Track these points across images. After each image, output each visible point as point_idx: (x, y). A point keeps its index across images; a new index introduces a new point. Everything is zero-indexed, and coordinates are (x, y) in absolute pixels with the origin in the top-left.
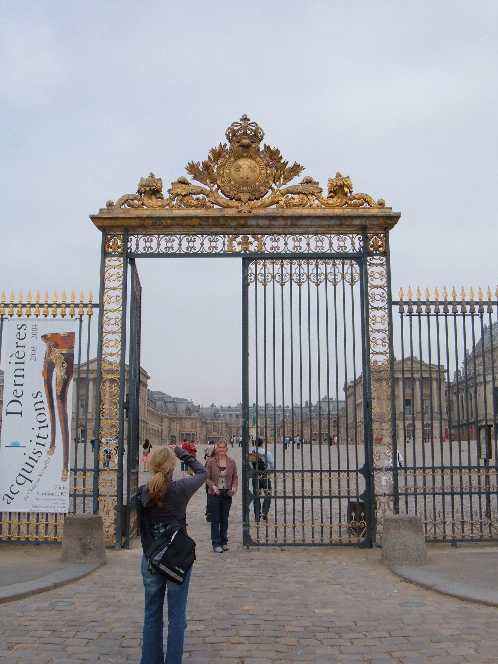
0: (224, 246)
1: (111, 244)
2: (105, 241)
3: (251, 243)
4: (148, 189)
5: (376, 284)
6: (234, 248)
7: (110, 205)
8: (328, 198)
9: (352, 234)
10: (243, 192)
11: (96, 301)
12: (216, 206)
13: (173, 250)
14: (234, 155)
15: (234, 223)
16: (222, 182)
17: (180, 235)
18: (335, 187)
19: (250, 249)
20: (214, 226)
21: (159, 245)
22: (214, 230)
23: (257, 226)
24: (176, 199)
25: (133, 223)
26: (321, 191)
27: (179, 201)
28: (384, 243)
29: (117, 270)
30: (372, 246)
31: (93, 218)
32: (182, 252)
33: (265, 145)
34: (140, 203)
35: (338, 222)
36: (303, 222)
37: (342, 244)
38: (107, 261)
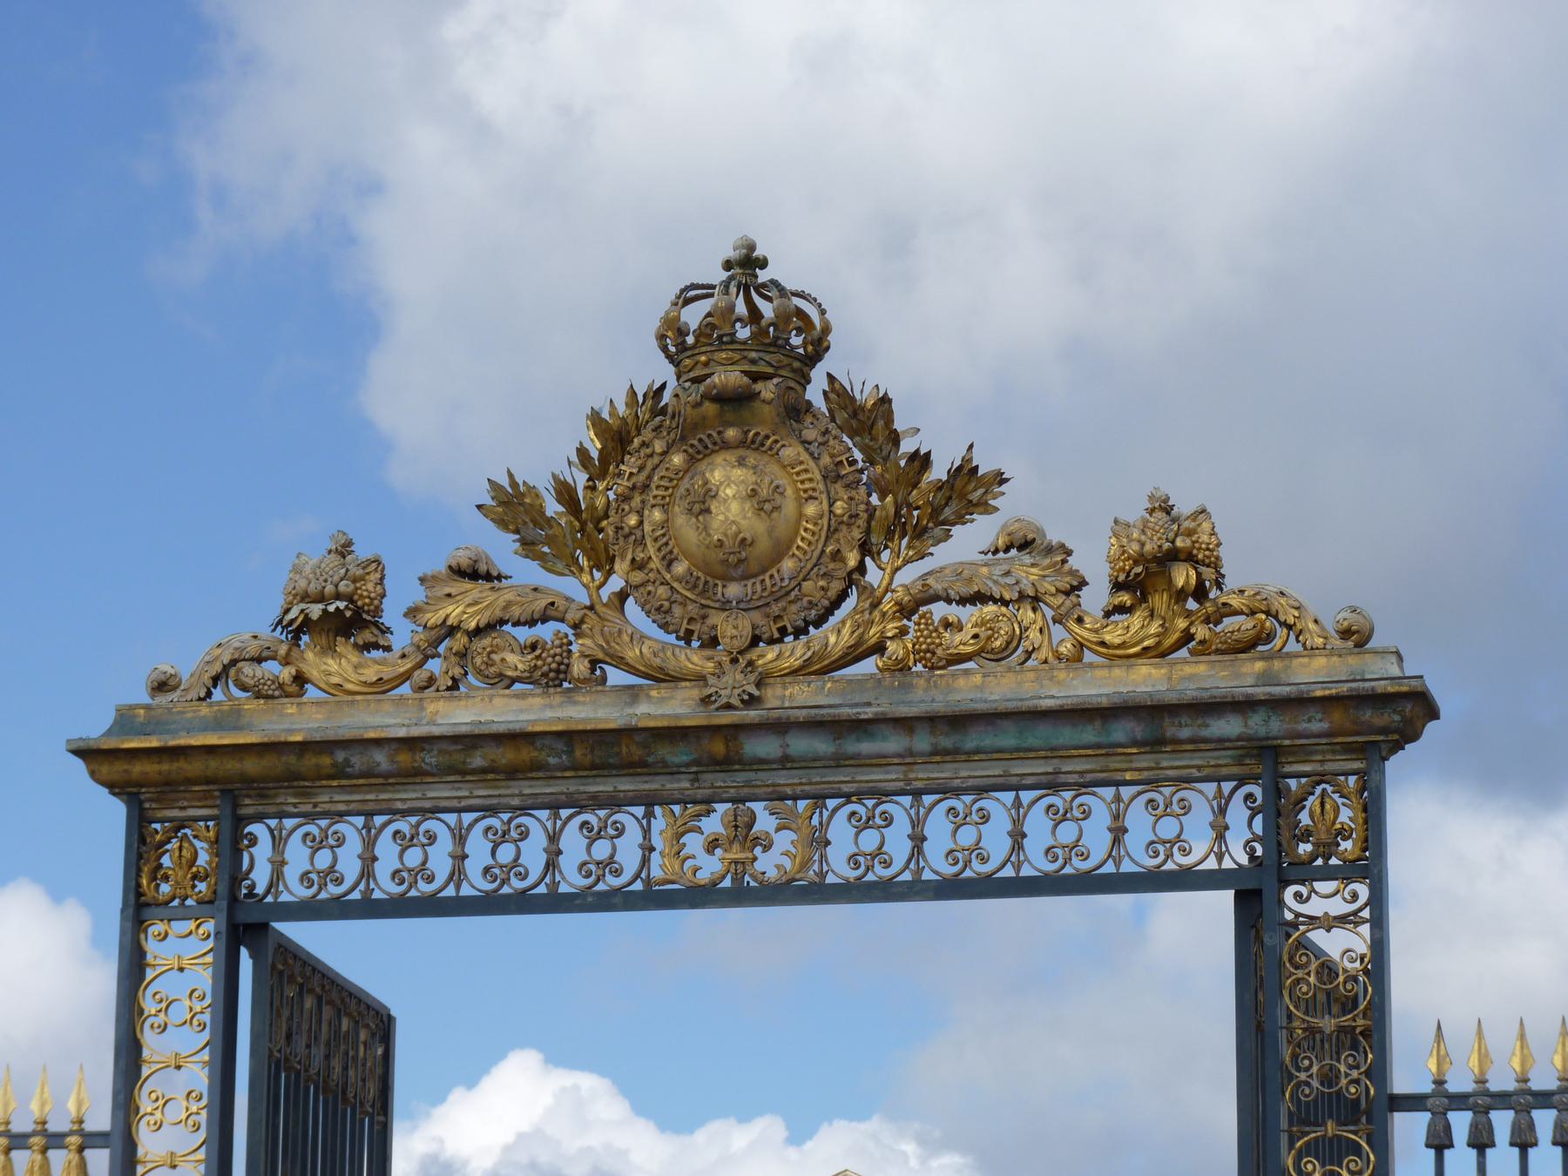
1: (166, 861)
2: (141, 849)
4: (315, 611)
6: (689, 863)
8: (1108, 614)
10: (725, 606)
11: (101, 1119)
14: (683, 438)
15: (678, 755)
16: (637, 565)
17: (459, 811)
18: (1136, 563)
19: (759, 866)
20: (599, 769)
22: (603, 787)
23: (785, 762)
24: (441, 649)
25: (251, 766)
27: (453, 659)
31: (86, 753)
33: (831, 378)
34: (286, 674)
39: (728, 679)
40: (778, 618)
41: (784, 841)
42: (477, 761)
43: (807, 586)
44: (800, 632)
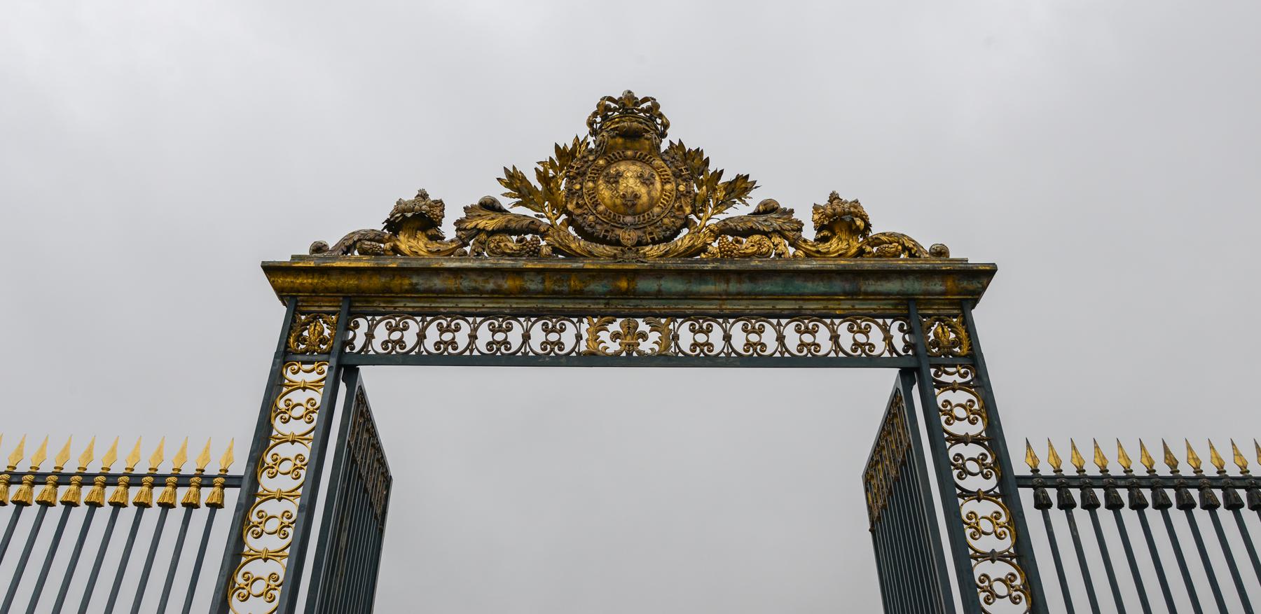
0: (578, 342)
2: (291, 327)
3: (644, 336)
7: (318, 248)
9: (884, 317)
10: (623, 226)
11: (239, 468)
13: (455, 349)
14: (605, 153)
25: (365, 282)
26: (799, 226)
28: (963, 334)
29: (309, 394)
30: (936, 343)
32: (476, 353)
34: (388, 246)
36: (767, 286)
40: (651, 233)
42: (490, 286)
43: (666, 220)
44: (660, 242)
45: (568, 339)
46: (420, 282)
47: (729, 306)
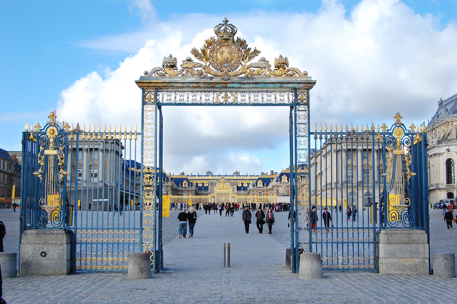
4: (169, 65)
5: (301, 122)
7: (146, 73)
10: (224, 67)
12: (209, 75)
21: (175, 98)
22: (208, 90)
24: (185, 70)
25: (160, 85)
33: (238, 37)
34: (164, 73)
35: (280, 85)
37: (282, 98)
38: (145, 107)
39: (225, 76)
41: (232, 98)
42: (192, 86)
45: (211, 98)
46: (175, 85)
47: (250, 90)
